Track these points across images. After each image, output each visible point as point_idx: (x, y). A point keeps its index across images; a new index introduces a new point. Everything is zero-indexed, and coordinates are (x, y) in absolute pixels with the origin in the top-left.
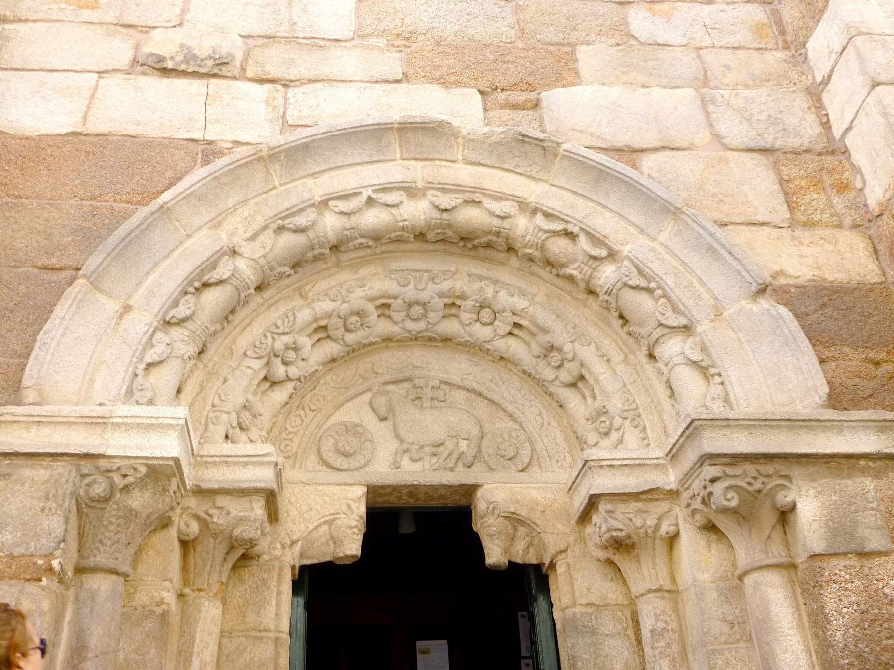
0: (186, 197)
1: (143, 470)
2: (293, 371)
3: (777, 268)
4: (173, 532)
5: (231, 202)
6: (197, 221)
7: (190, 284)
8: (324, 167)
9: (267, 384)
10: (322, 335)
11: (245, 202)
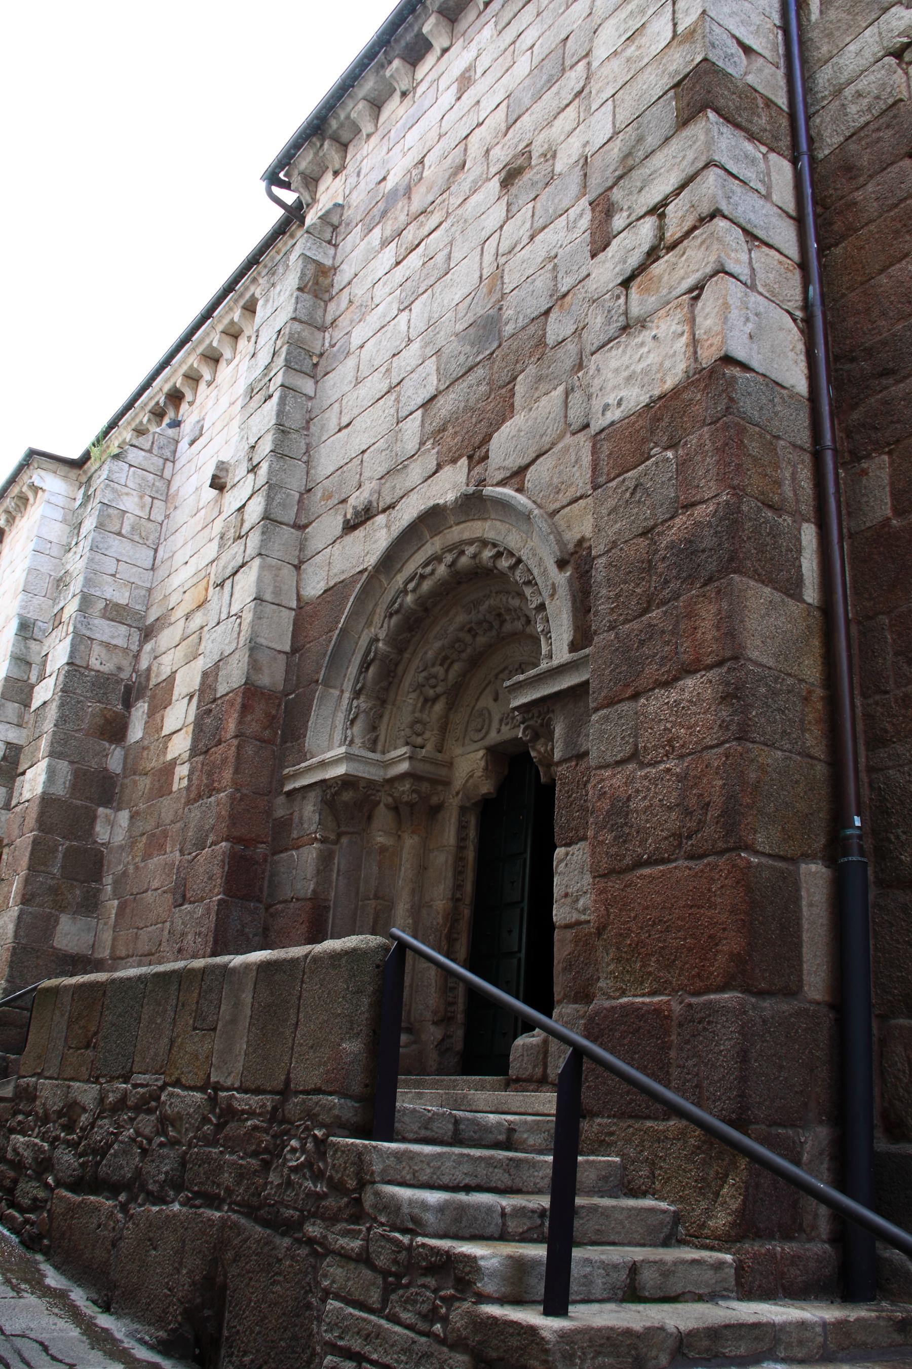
0: (349, 617)
1: (340, 782)
2: (439, 689)
3: (579, 536)
4: (382, 805)
5: (370, 607)
6: (360, 627)
7: (362, 667)
8: (401, 564)
9: (429, 704)
10: (449, 661)
11: (376, 605)
